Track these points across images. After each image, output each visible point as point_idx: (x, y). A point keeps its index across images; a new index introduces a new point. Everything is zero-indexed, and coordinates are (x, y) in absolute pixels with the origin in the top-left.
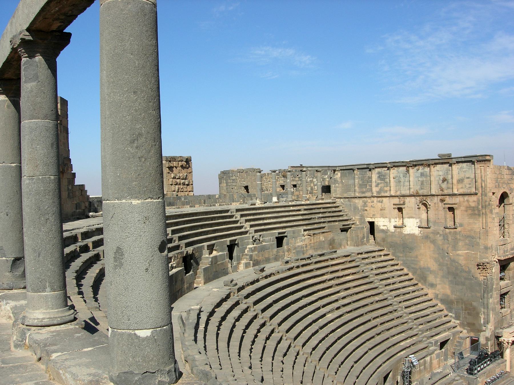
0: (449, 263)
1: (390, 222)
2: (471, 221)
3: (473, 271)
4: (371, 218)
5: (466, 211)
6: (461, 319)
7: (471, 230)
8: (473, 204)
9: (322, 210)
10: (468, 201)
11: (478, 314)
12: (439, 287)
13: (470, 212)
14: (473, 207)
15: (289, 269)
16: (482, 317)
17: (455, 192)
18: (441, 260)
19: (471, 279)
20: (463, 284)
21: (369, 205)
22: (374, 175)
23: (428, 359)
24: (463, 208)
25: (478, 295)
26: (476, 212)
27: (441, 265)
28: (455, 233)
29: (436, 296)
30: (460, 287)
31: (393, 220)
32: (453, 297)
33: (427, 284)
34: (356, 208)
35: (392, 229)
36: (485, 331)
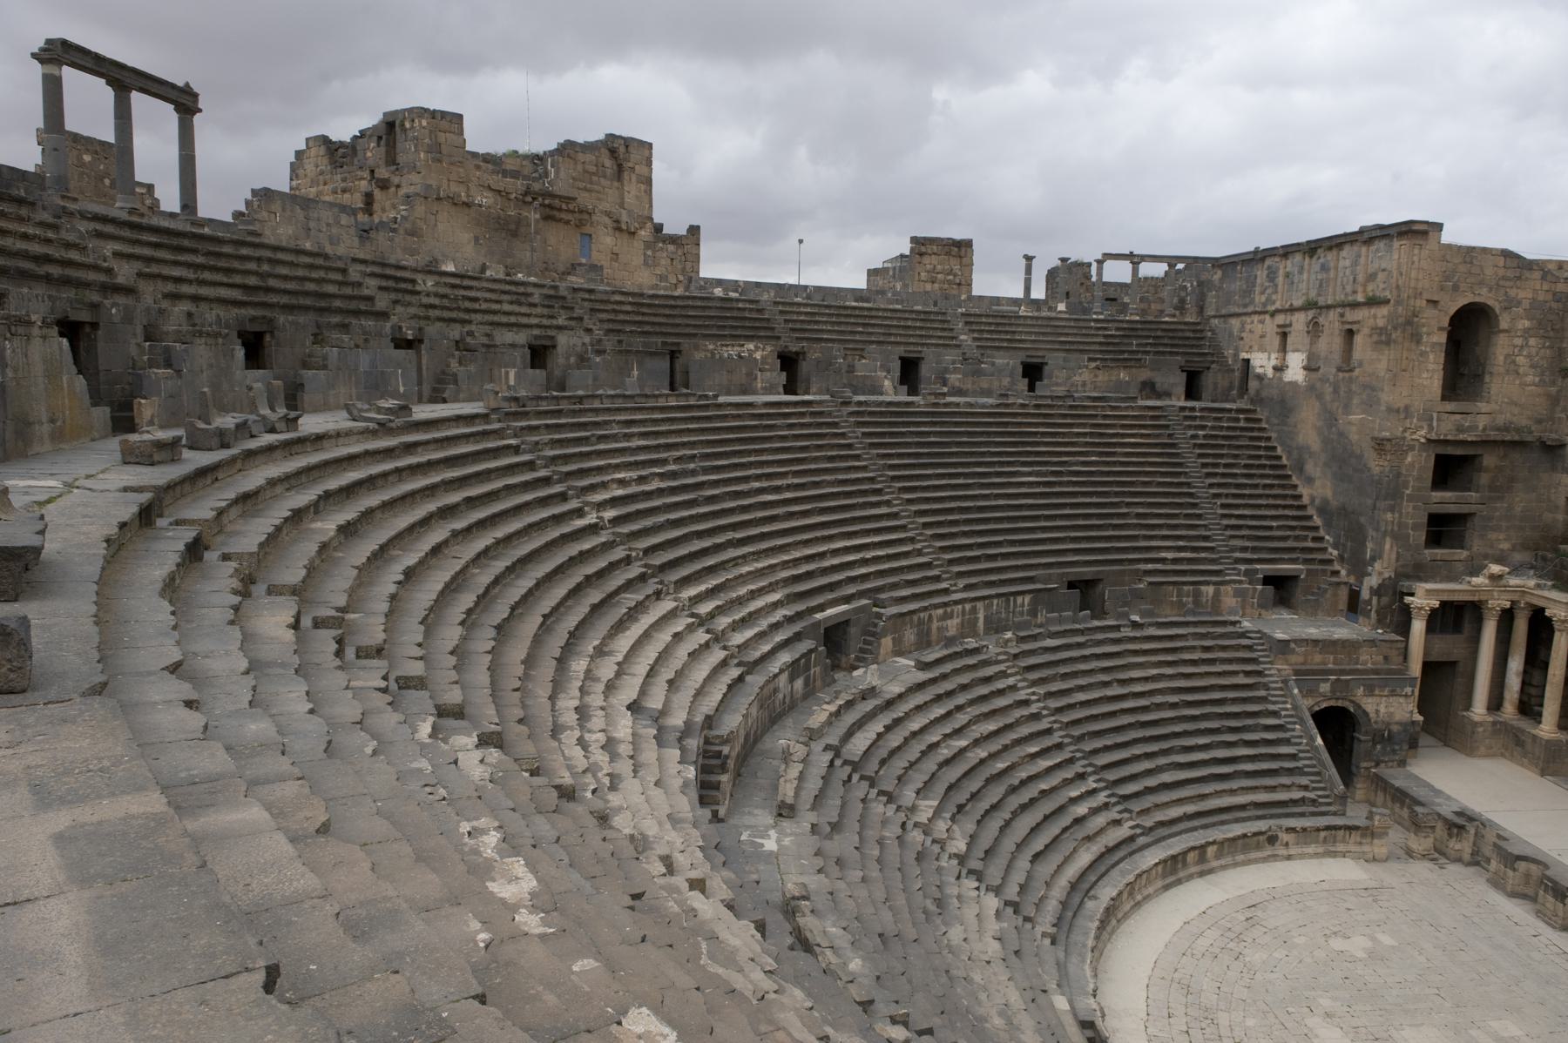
8: (1381, 323)
9: (1159, 333)
10: (1375, 317)
12: (1318, 483)
15: (998, 406)
16: (1370, 545)
17: (1360, 298)
21: (1248, 327)
22: (1261, 274)
23: (1210, 589)
24: (1366, 331)
25: (1369, 502)
28: (1351, 380)
29: (1313, 499)
31: (1273, 356)
32: (1334, 504)
34: (1231, 334)
35: (1270, 373)
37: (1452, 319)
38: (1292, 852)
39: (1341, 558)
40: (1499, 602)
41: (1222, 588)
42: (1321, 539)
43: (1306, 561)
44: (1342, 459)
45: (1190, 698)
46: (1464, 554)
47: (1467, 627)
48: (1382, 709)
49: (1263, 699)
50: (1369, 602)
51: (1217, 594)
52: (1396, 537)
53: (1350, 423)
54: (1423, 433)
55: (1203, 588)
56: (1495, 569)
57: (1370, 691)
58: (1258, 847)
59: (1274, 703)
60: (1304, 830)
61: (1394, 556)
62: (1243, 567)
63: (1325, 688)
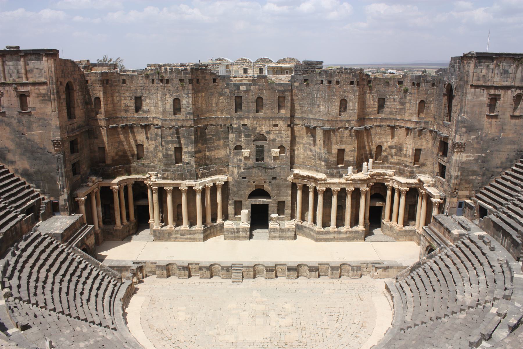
0: (25, 142)
2: (42, 105)
3: (47, 147)
5: (38, 97)
6: (41, 187)
7: (44, 113)
8: (43, 92)
10: (39, 89)
11: (56, 181)
13: (41, 98)
14: (44, 94)
18: (18, 140)
19: (47, 154)
20: (40, 159)
23: (18, 225)
25: (55, 166)
26: (47, 98)
27: (19, 145)
29: (16, 171)
30: (38, 161)
32: (32, 170)
36: (63, 195)
37: (66, 88)
39: (44, 193)
42: (29, 187)
43: (33, 198)
44: (31, 151)
45: (62, 272)
46: (80, 176)
49: (73, 260)
50: (65, 205)
53: (33, 135)
56: (94, 178)
57: (87, 239)
62: (20, 210)
63: (80, 244)
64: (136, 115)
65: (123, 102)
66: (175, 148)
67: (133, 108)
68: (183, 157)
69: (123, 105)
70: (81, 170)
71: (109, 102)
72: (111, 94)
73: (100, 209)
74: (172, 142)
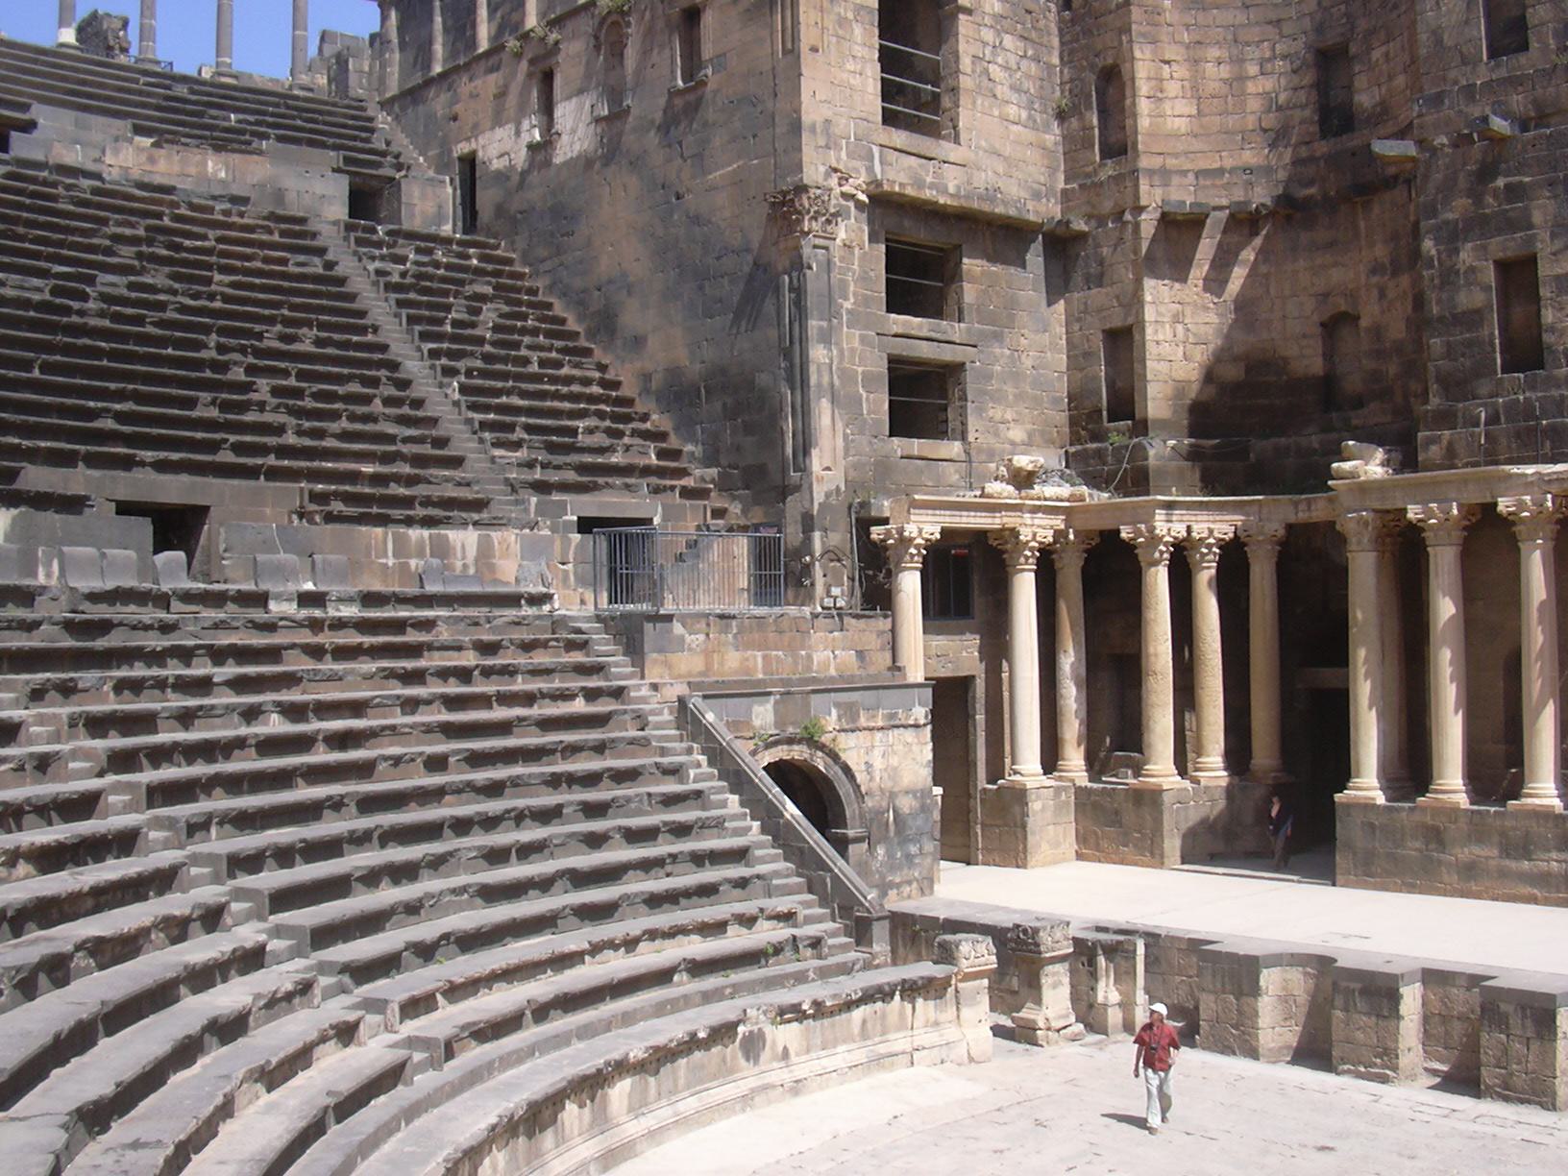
1: (518, 133)
4: (468, 139)
12: (653, 343)
16: (789, 426)
18: (660, 232)
31: (526, 125)
32: (694, 369)
33: (619, 342)
36: (798, 488)
38: (800, 1072)
40: (1036, 530)
41: (496, 535)
46: (955, 448)
47: (979, 602)
48: (878, 763)
51: (485, 551)
52: (834, 400)
54: (862, 179)
55: (453, 535)
58: (726, 1072)
59: (663, 752)
60: (820, 1010)
61: (840, 442)
64: (1322, 148)
65: (1251, 87)
66: (1502, 266)
67: (1307, 113)
68: (1548, 316)
69: (1254, 105)
70: (973, 423)
71: (1173, 88)
72: (1188, 47)
73: (1069, 660)
74: (1478, 226)
